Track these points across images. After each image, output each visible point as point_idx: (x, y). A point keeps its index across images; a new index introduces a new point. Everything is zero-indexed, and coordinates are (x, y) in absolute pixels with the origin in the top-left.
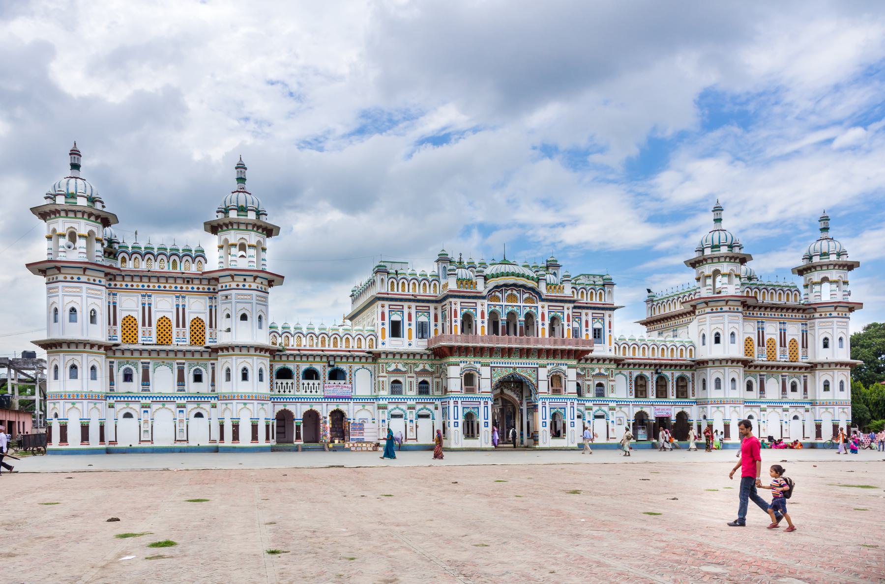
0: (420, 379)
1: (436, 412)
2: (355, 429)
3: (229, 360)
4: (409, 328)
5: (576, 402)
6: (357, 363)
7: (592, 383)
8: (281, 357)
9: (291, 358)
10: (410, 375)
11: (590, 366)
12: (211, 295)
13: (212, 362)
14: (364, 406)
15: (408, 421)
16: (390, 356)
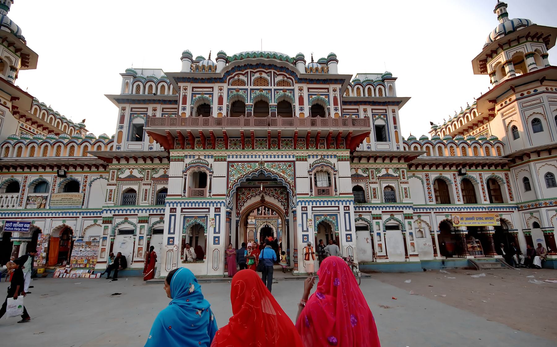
0: (159, 187)
5: (352, 206)
6: (94, 172)
10: (146, 182)
14: (95, 221)
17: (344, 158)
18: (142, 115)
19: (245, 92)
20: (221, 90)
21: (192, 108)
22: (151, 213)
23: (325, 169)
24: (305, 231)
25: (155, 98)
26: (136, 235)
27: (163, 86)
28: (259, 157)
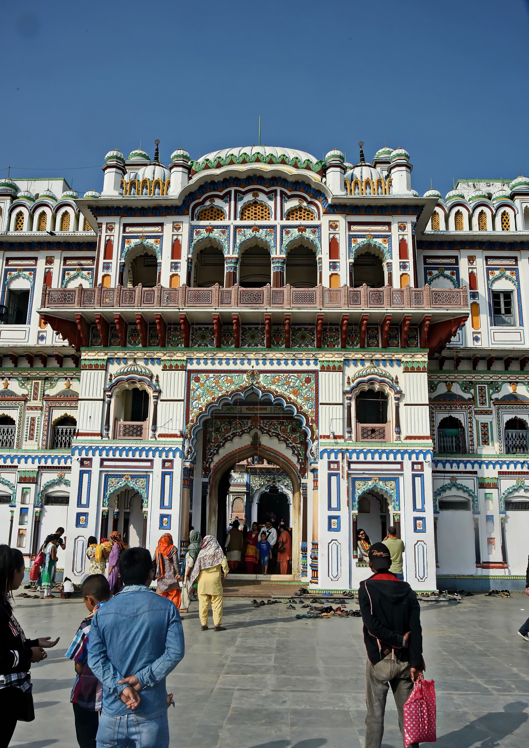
0: (57, 414)
7: (496, 420)
11: (487, 378)
17: (416, 366)
18: (27, 273)
19: (223, 232)
21: (123, 266)
22: (43, 464)
23: (377, 387)
24: (335, 509)
25: (52, 239)
26: (15, 506)
28: (249, 364)
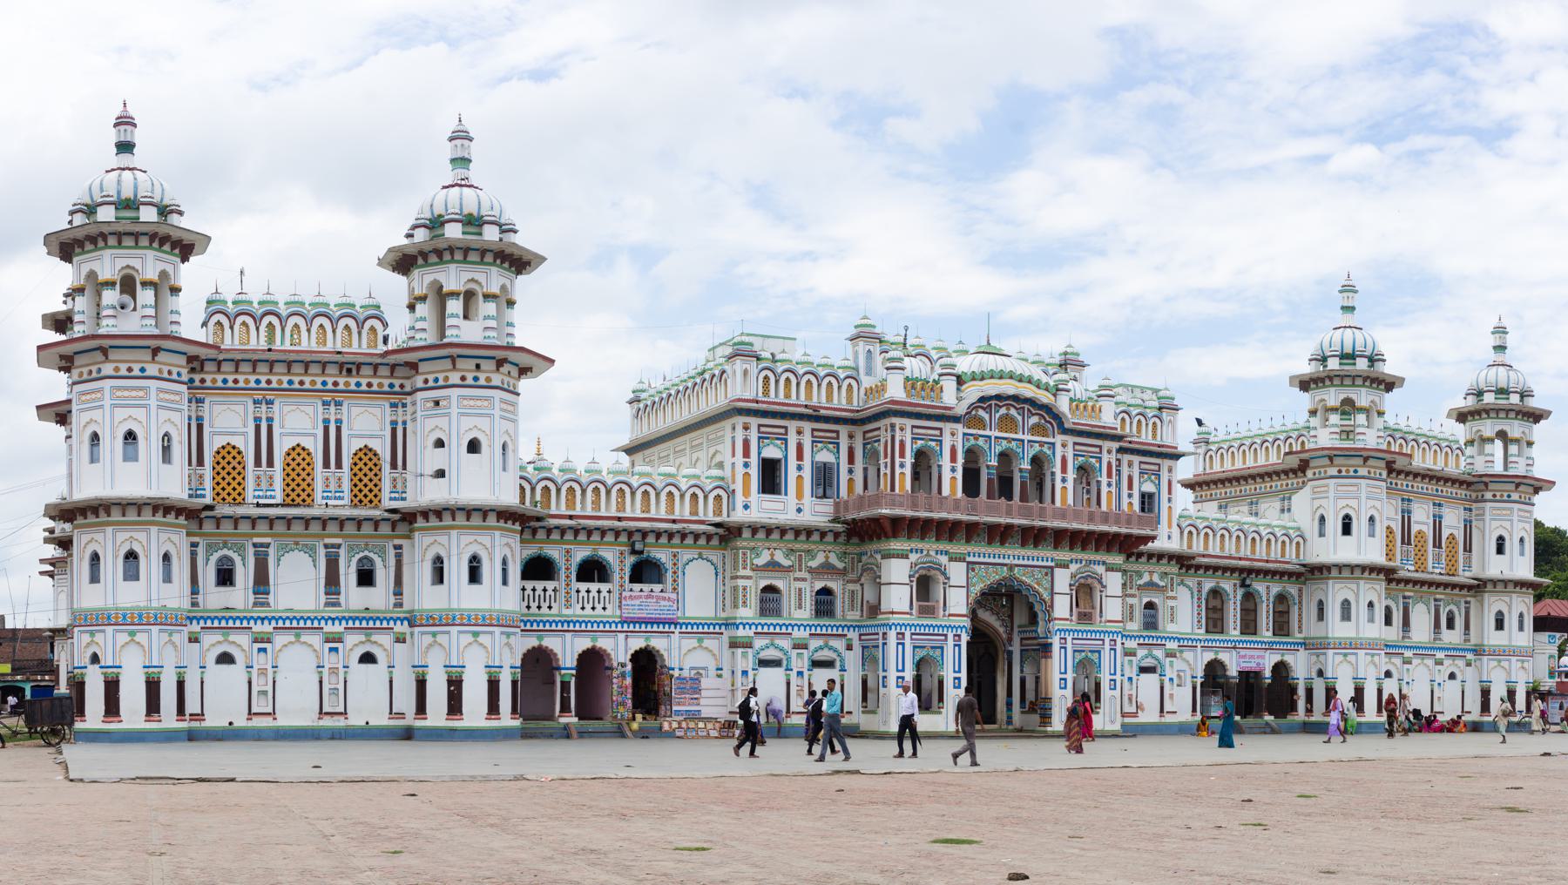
0: (819, 585)
1: (849, 655)
2: (682, 691)
3: (443, 539)
4: (797, 475)
6: (688, 547)
8: (534, 531)
9: (555, 536)
10: (798, 574)
12: (395, 399)
13: (397, 542)
14: (700, 640)
15: (793, 674)
16: (761, 535)
20: (953, 434)
27: (809, 381)
